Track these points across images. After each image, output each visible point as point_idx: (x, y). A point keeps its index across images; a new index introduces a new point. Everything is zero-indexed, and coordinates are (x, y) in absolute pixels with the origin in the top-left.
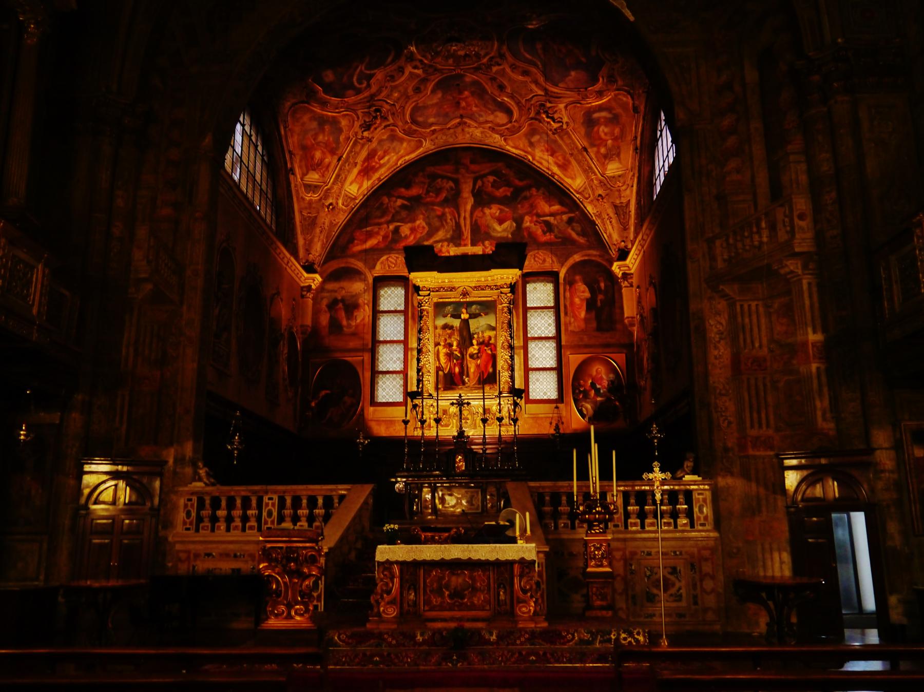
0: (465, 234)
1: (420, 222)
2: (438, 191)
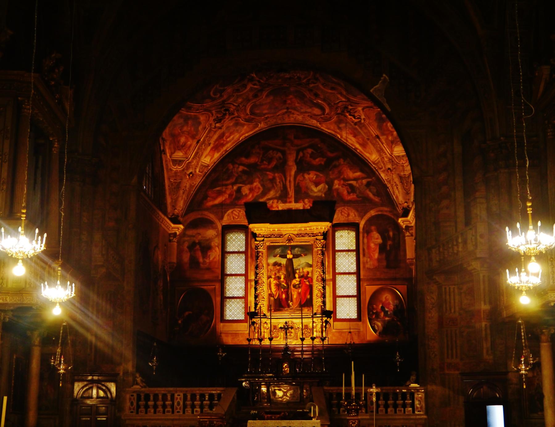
2: (270, 160)
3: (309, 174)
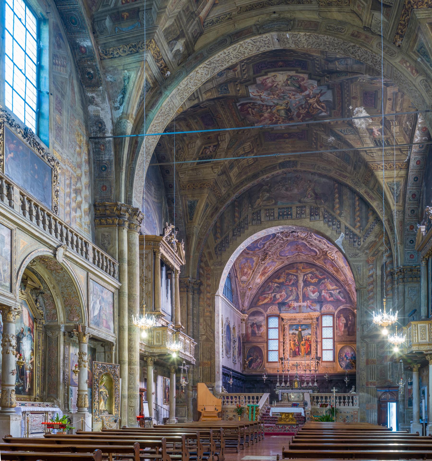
1: (284, 293)
2: (290, 280)
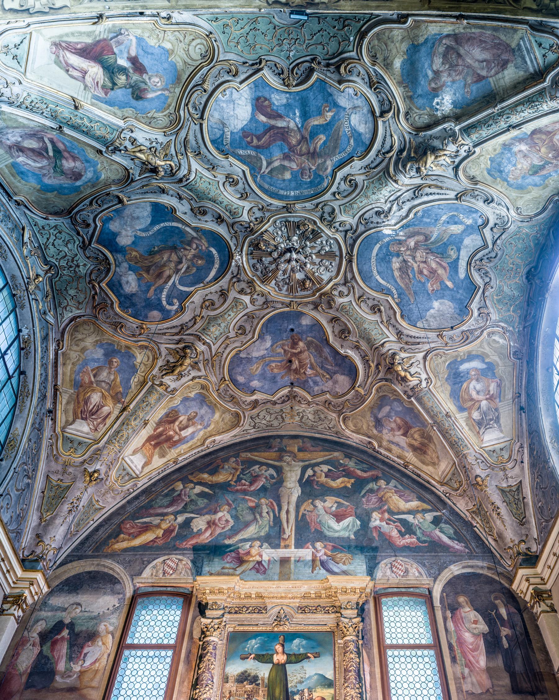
0: (288, 532)
1: (223, 515)
2: (254, 479)
3: (325, 501)
